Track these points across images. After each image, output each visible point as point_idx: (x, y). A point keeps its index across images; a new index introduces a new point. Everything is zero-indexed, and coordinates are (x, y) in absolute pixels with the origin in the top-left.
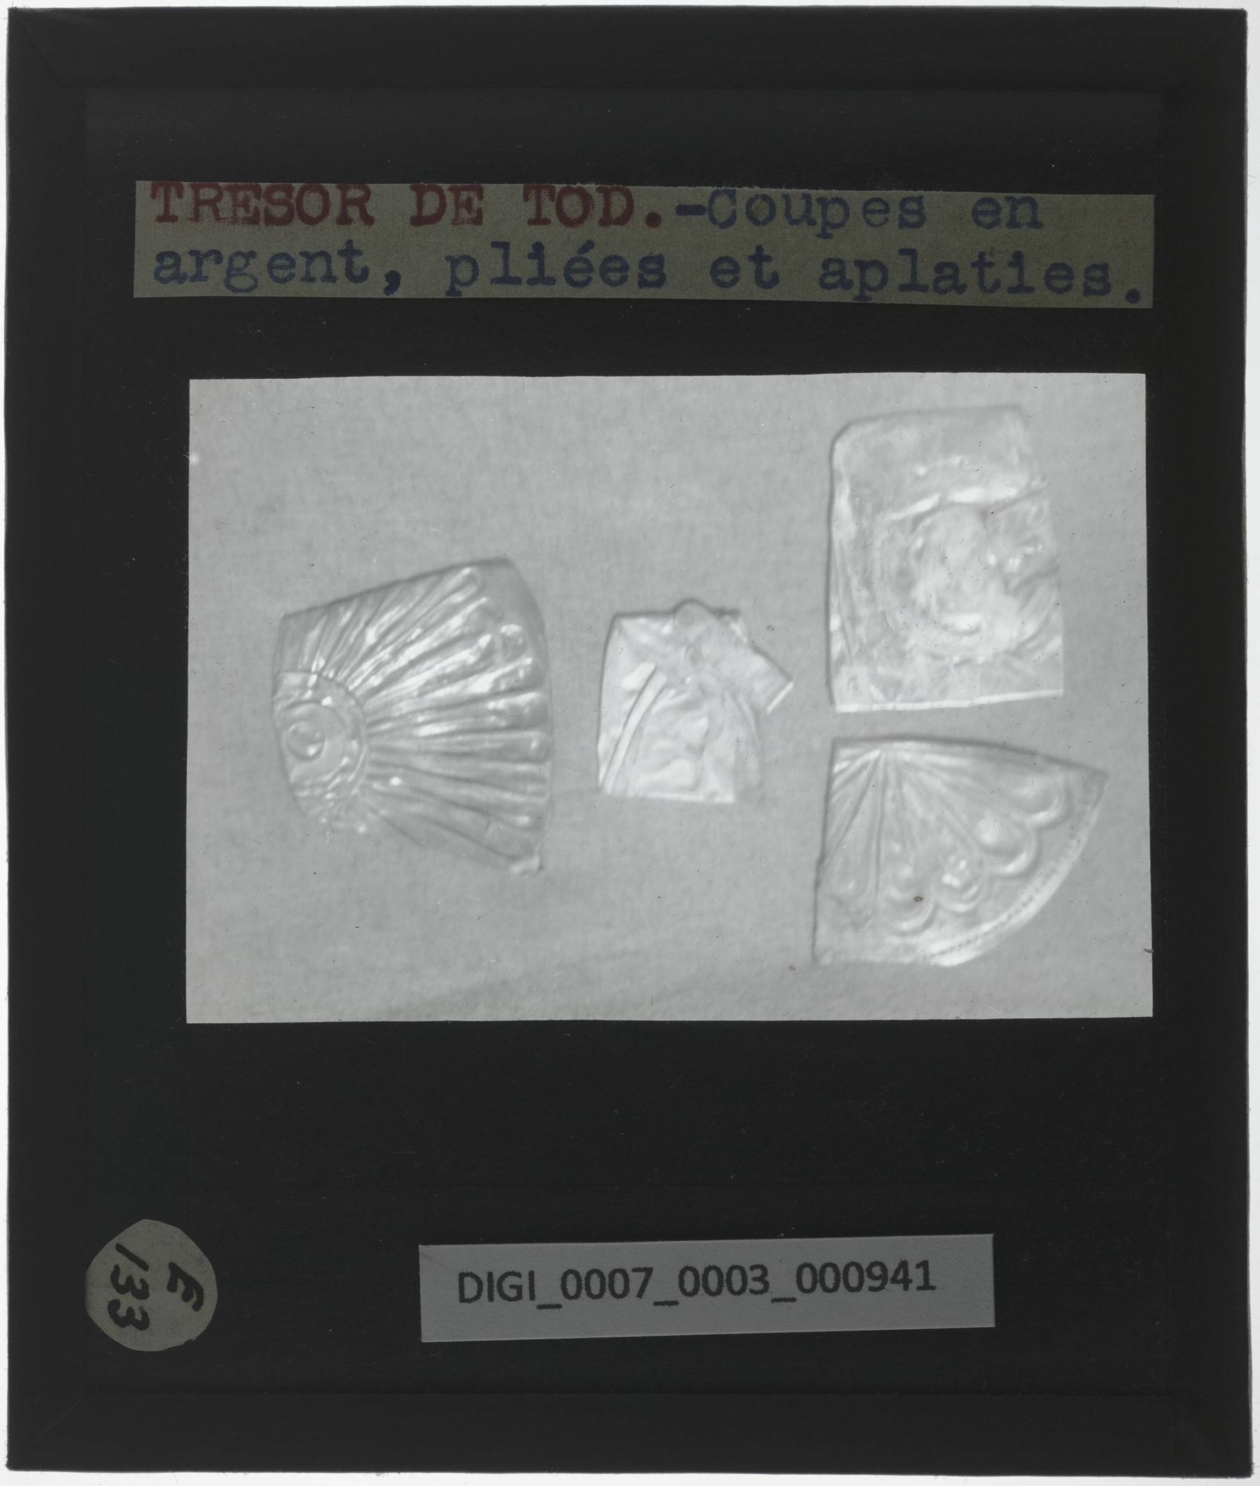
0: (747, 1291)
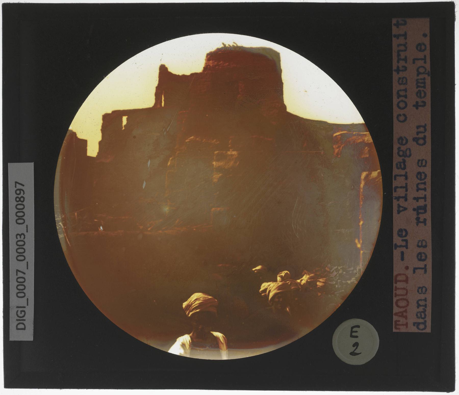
0: (24, 240)
